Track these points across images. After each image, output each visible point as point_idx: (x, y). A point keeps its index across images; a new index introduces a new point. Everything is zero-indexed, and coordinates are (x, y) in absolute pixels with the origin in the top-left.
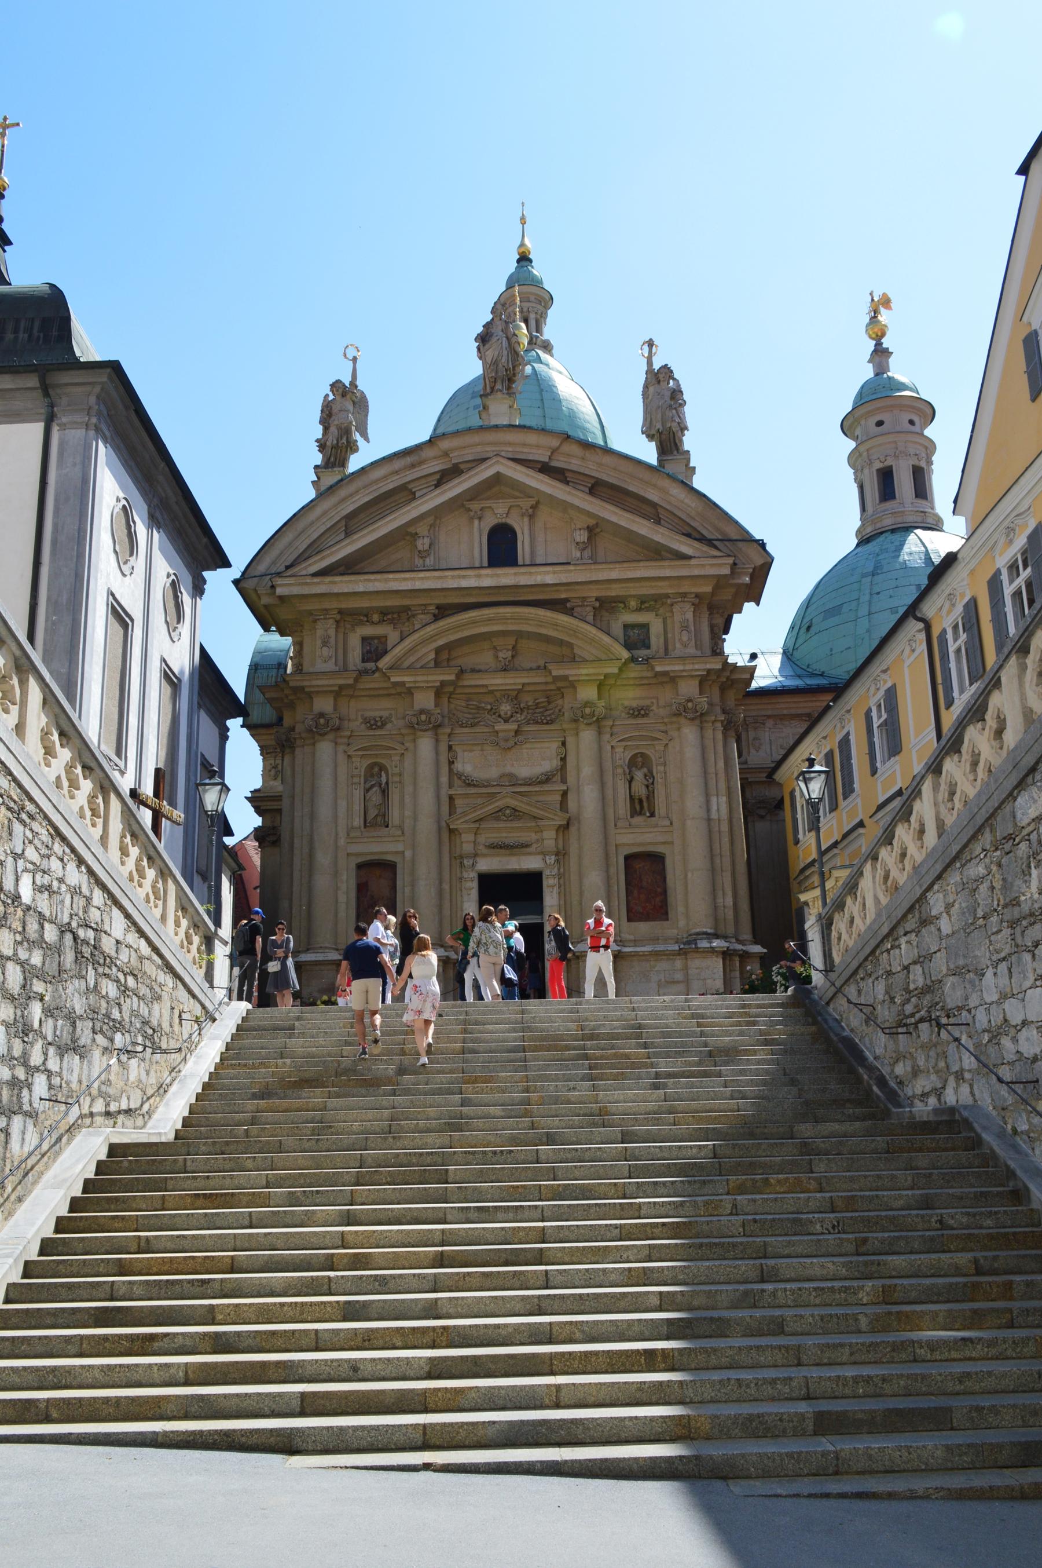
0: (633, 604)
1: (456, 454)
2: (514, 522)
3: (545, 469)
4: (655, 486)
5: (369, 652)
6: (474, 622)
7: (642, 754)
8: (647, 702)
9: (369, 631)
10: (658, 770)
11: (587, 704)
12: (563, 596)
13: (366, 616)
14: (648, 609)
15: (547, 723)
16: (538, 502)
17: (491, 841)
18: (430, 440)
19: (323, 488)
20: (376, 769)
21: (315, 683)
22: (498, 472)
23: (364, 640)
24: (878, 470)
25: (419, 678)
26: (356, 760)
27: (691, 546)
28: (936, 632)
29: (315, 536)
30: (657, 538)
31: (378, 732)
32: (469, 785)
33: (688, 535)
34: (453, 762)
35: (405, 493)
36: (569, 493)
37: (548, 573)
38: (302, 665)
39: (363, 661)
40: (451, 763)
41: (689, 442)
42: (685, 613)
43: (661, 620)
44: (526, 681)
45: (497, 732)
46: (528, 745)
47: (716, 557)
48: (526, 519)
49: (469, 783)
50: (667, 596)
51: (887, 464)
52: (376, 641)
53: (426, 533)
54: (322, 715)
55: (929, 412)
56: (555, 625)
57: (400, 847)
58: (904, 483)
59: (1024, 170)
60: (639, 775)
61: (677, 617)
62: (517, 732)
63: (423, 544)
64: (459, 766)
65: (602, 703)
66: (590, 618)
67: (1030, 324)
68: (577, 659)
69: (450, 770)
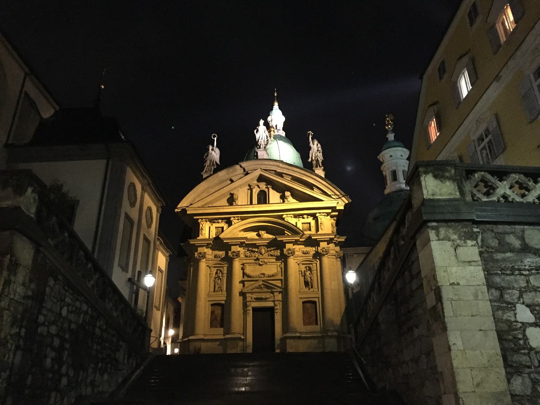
7: (308, 267)
17: (257, 296)
23: (216, 228)
24: (391, 171)
49: (249, 276)
68: (286, 235)
69: (244, 273)
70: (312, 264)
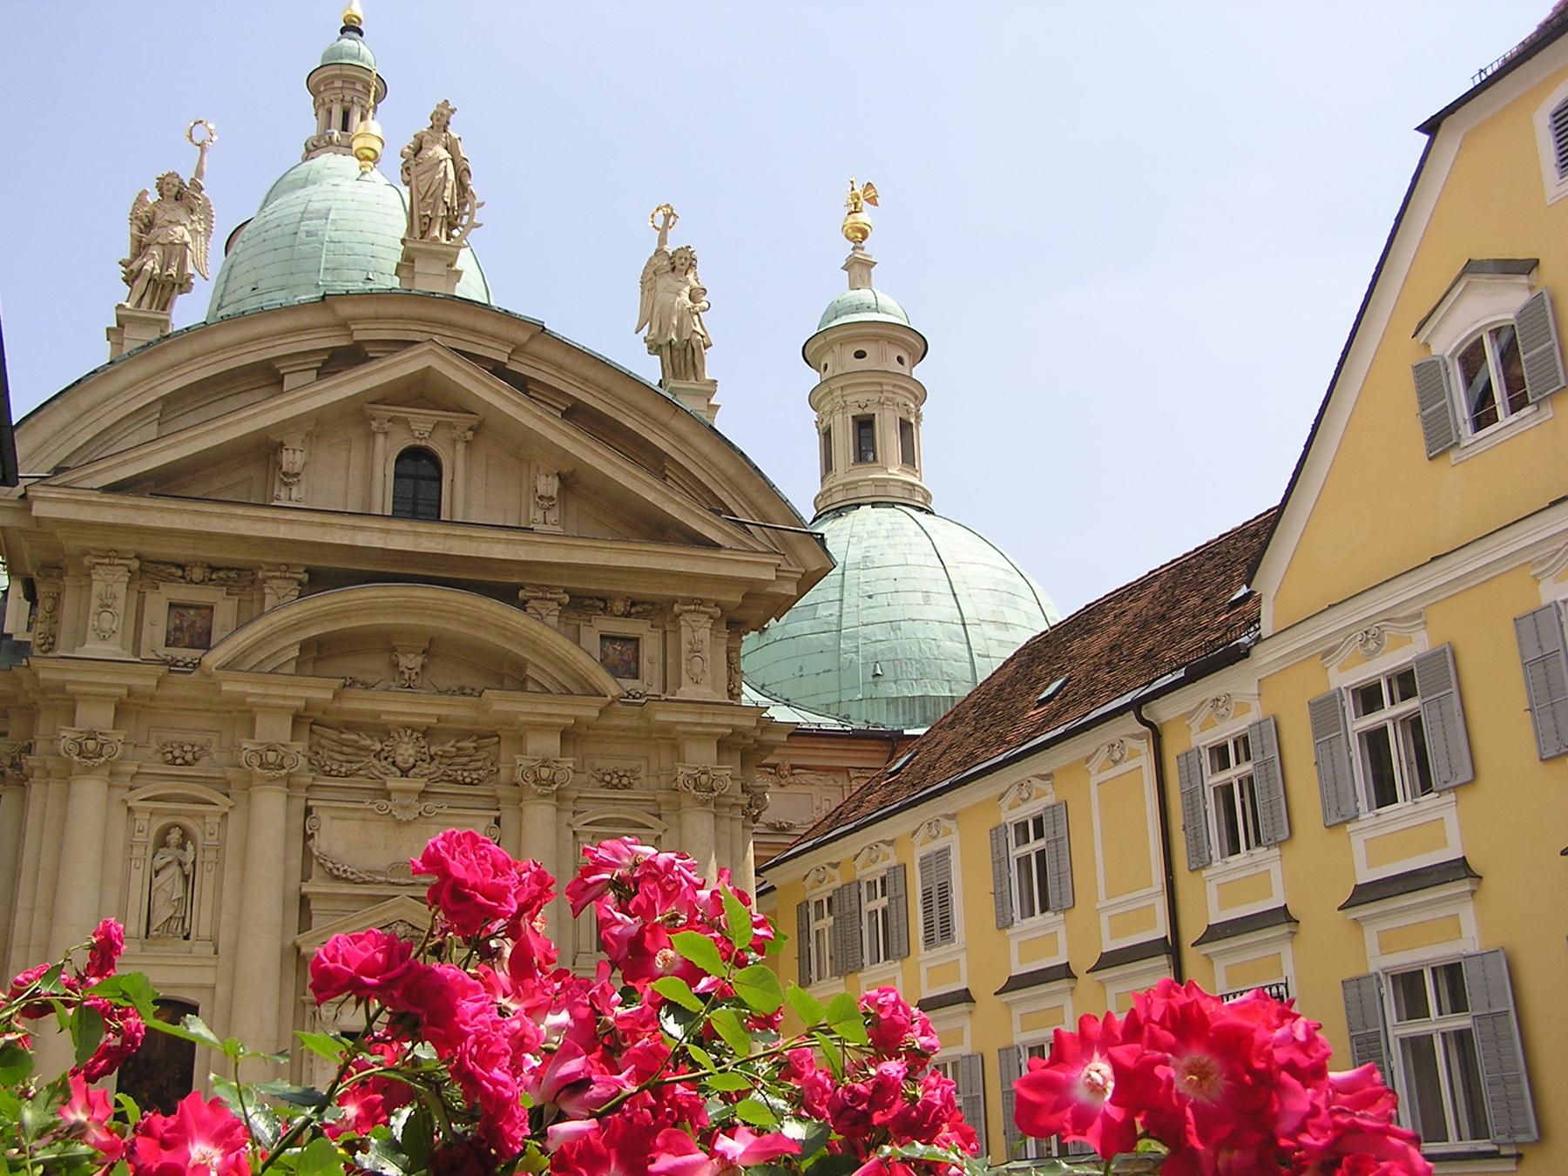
0: (619, 606)
1: (360, 327)
3: (499, 370)
4: (665, 427)
5: (176, 629)
6: (371, 608)
8: (633, 764)
9: (183, 593)
11: (545, 763)
12: (516, 580)
13: (184, 571)
14: (638, 615)
15: (471, 784)
16: (481, 424)
18: (323, 297)
19: (129, 346)
20: (175, 836)
21: (84, 678)
22: (429, 367)
23: (171, 605)
24: (853, 417)
25: (272, 691)
26: (142, 819)
27: (719, 529)
29: (106, 422)
30: (670, 509)
31: (186, 771)
32: (337, 878)
33: (718, 513)
34: (312, 835)
35: (268, 376)
36: (540, 418)
37: (499, 541)
38: (54, 637)
39: (167, 645)
40: (308, 837)
41: (712, 366)
42: (697, 631)
43: (658, 633)
44: (444, 711)
45: (387, 795)
46: (440, 819)
47: (757, 552)
48: (460, 447)
51: (867, 411)
52: (192, 612)
53: (298, 446)
54: (91, 735)
56: (503, 630)
57: (208, 977)
58: (888, 439)
61: (686, 634)
62: (424, 794)
63: (291, 459)
64: (320, 844)
65: (569, 763)
66: (553, 620)
67: (1427, 345)
68: (531, 686)
69: (307, 853)
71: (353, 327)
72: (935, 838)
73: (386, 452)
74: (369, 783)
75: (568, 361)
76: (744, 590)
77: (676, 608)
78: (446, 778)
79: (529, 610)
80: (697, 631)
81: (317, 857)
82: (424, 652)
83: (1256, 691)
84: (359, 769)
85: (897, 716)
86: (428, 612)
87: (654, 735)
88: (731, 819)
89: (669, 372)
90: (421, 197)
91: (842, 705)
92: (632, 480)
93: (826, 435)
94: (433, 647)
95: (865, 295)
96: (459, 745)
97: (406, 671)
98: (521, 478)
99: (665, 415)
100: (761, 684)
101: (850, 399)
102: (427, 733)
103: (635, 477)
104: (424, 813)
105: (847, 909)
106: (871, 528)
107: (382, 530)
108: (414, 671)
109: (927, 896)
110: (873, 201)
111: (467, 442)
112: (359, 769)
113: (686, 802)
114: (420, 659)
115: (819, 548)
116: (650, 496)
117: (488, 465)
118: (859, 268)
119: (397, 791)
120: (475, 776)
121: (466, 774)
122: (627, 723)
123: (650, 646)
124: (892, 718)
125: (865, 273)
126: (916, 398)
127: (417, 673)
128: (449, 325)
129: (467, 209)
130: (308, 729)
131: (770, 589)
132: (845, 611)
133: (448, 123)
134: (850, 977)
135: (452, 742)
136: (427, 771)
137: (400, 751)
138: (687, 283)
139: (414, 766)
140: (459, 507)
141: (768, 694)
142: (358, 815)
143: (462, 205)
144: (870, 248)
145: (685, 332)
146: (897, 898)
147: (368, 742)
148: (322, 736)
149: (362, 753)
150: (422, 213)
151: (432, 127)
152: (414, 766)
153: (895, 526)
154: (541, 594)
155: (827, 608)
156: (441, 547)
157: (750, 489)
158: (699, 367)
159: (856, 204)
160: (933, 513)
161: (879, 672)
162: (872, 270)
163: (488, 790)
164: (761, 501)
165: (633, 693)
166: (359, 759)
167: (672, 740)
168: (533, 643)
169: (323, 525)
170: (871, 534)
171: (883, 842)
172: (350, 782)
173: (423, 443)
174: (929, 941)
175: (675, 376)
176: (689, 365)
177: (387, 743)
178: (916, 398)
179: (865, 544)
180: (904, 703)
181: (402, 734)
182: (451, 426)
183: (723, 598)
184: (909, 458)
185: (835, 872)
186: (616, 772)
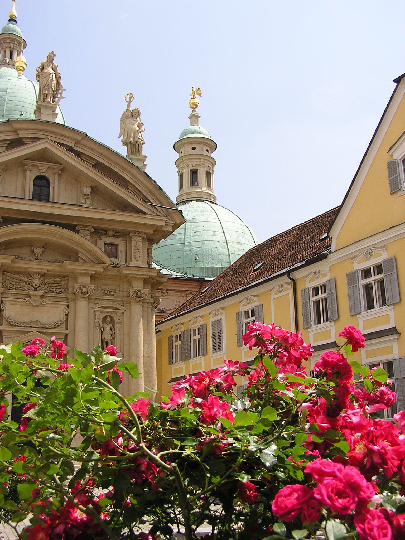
0: (111, 233)
1: (21, 132)
2: (49, 175)
3: (71, 149)
4: (128, 171)
6: (25, 231)
8: (114, 288)
10: (118, 326)
11: (85, 287)
14: (118, 236)
15: (59, 293)
16: (64, 168)
18: (8, 121)
24: (191, 170)
28: (300, 288)
30: (129, 200)
32: (12, 325)
33: (146, 202)
36: (85, 167)
37: (70, 209)
42: (138, 242)
44: (49, 268)
46: (48, 305)
48: (57, 176)
50: (130, 232)
51: (195, 168)
55: (215, 147)
56: (71, 240)
58: (202, 178)
59: (397, 81)
60: (108, 327)
61: (134, 243)
62: (42, 296)
65: (93, 287)
66: (88, 237)
67: (392, 155)
68: (80, 260)
70: (116, 313)
71: (19, 132)
72: (217, 315)
73: (30, 176)
74: (24, 292)
75: (95, 147)
76: (155, 229)
77: (131, 234)
78: (50, 291)
79: (80, 234)
80: (138, 242)
81: (5, 318)
82: (43, 247)
83: (329, 270)
84: (20, 287)
85: (203, 274)
86: (45, 233)
87: (122, 278)
88: (148, 307)
89: (130, 152)
90: (43, 86)
91: (185, 269)
92: (117, 190)
93: (181, 176)
94: (46, 246)
95: (196, 128)
96: (55, 280)
97: (37, 254)
98: (77, 188)
99: (128, 168)
100: (156, 261)
101: (190, 164)
102: (44, 275)
103: (118, 189)
104: (42, 303)
105: (186, 339)
106: (196, 209)
107: (29, 204)
108: (39, 254)
109: (214, 335)
110: (200, 95)
111: (59, 174)
112: (20, 287)
113: (132, 301)
114: (41, 250)
115: (180, 215)
116: (123, 195)
117: (66, 183)
118: (194, 118)
119: (32, 295)
120: (60, 291)
121: (57, 290)
122: (113, 273)
123: (121, 247)
124: (202, 275)
125: (196, 120)
126: (212, 164)
127: (40, 255)
128: (53, 133)
129: (60, 91)
130: (2, 273)
131: (163, 229)
132: (186, 237)
133: (53, 59)
134: (186, 362)
135: (52, 279)
136: (43, 289)
137: (34, 281)
138: (137, 121)
139: (39, 287)
140: (56, 197)
141: (159, 264)
142: (20, 303)
143: (58, 90)
144: (198, 111)
145: (136, 139)
146: (203, 335)
147: (23, 278)
148: (7, 276)
149: (20, 282)
150: (44, 92)
151: (47, 61)
152: (39, 287)
153: (204, 208)
154: (84, 228)
155: (180, 236)
156: (49, 211)
157: (157, 194)
158: (140, 151)
159: (194, 95)
160: (217, 204)
161: (197, 258)
162: (199, 119)
163: (64, 295)
164: (161, 198)
165: (115, 263)
166: (20, 284)
167: (128, 280)
168: (81, 245)
169: (8, 202)
170: (196, 211)
171: (199, 316)
172: (16, 292)
173: (43, 174)
174: (214, 350)
175: (132, 153)
176: (137, 150)
177: (30, 279)
178: (212, 164)
179: (194, 214)
180: (206, 269)
181: (35, 275)
182: (53, 169)
183: (146, 231)
184: (209, 185)
185: (182, 326)
186: (108, 290)
